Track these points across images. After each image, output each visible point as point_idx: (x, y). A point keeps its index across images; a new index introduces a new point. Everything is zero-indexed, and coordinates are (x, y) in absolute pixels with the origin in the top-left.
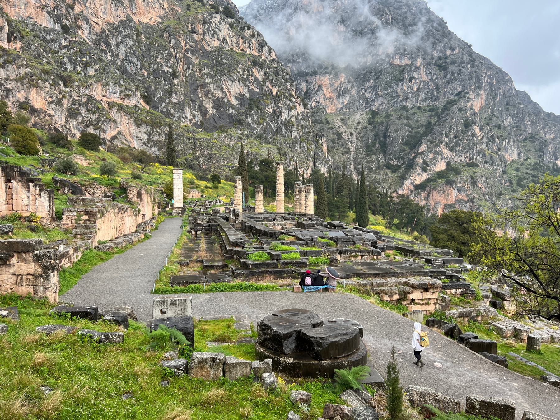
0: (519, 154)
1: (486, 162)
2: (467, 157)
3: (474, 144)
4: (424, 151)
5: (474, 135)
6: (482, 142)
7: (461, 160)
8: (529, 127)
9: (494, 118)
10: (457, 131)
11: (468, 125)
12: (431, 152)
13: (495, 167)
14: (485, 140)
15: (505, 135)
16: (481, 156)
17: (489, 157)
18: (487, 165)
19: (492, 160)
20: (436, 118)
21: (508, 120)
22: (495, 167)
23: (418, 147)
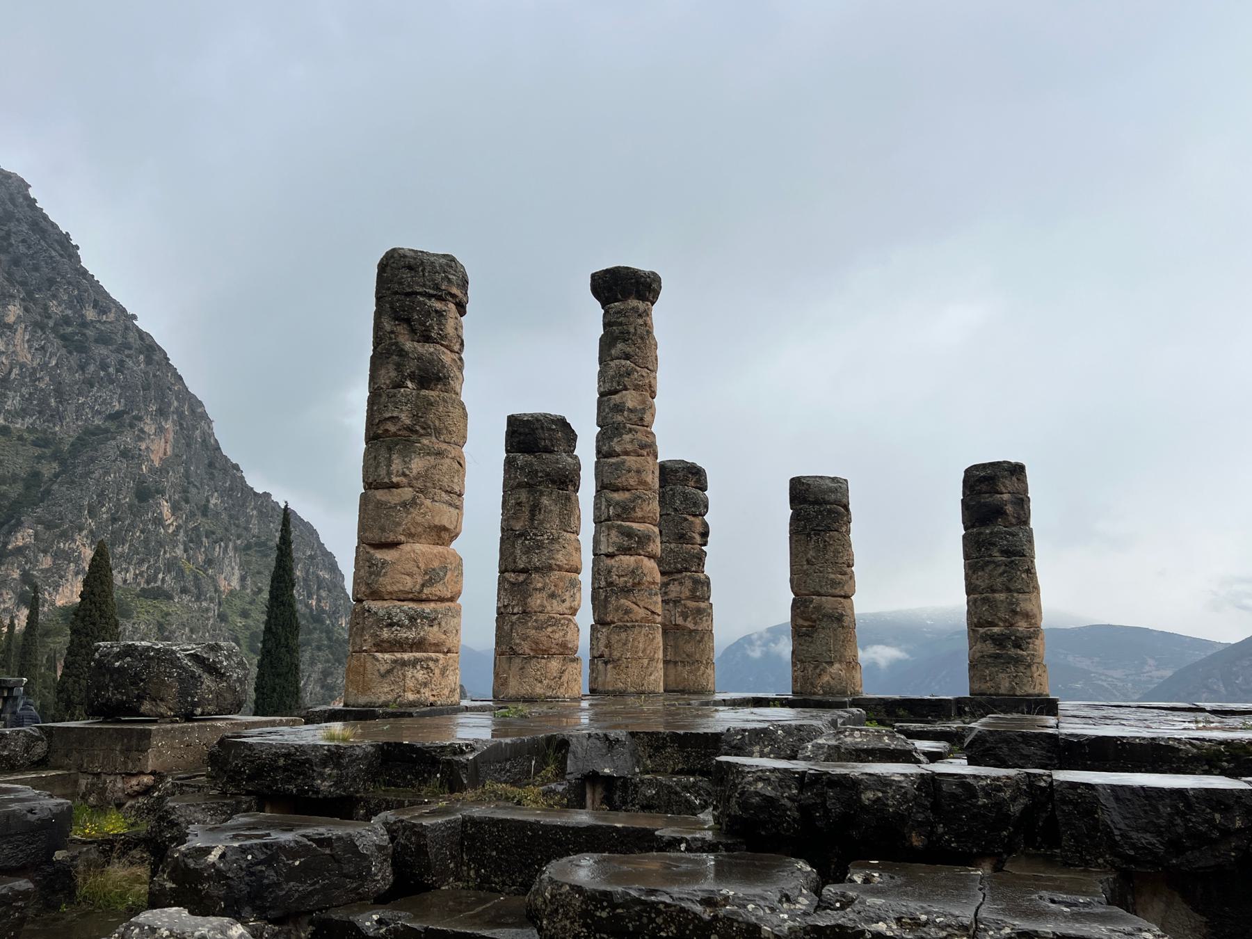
0: (243, 579)
1: (184, 591)
2: (141, 574)
3: (161, 544)
4: (26, 547)
5: (159, 521)
6: (177, 541)
7: (125, 581)
8: (255, 521)
9: (193, 490)
10: (118, 505)
11: (144, 494)
12: (45, 552)
13: (204, 604)
14: (181, 536)
15: (220, 533)
16: (173, 574)
17: (191, 578)
18: (186, 598)
19: (198, 587)
20: (55, 465)
21: (213, 501)
22: (204, 604)
23: (9, 533)
